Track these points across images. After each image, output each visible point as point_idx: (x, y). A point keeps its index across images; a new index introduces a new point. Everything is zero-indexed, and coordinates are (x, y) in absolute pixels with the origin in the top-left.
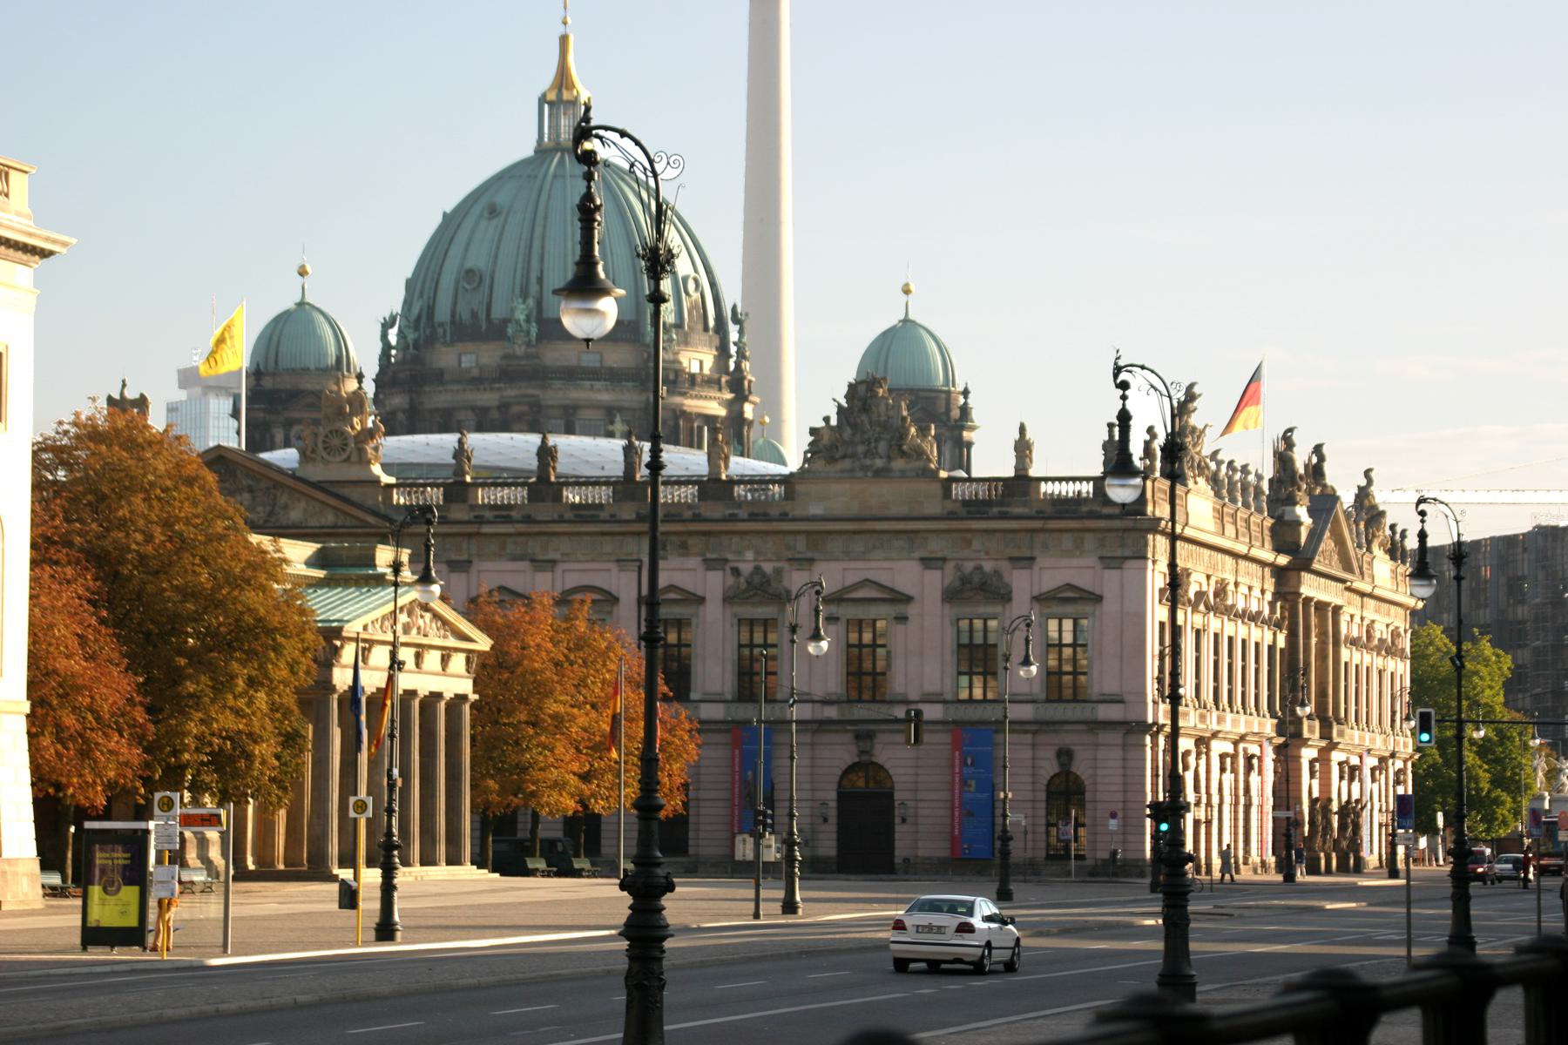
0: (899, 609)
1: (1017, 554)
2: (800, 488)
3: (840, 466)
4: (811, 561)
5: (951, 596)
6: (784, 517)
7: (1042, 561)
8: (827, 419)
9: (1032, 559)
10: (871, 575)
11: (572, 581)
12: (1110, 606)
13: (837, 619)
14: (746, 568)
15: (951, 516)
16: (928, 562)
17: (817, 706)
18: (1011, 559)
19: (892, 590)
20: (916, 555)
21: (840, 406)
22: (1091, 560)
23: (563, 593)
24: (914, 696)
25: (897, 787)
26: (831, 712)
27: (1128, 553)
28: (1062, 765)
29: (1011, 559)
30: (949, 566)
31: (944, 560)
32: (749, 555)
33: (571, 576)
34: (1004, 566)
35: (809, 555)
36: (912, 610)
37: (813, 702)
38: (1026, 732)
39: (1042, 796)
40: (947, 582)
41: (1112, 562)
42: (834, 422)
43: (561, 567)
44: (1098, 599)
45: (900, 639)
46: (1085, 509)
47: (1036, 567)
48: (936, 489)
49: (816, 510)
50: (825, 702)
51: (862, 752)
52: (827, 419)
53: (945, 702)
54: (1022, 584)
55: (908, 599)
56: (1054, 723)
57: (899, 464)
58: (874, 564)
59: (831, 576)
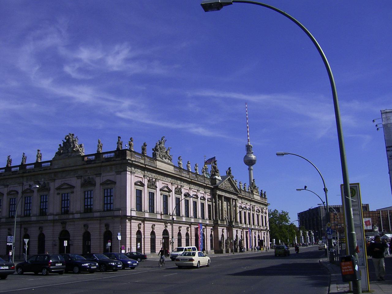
1: (98, 173)
2: (53, 162)
4: (55, 180)
5: (83, 185)
6: (50, 169)
7: (103, 175)
8: (60, 145)
9: (101, 174)
10: (66, 182)
11: (11, 189)
12: (118, 184)
13: (59, 194)
14: (42, 183)
15: (84, 164)
16: (78, 177)
17: (54, 216)
18: (96, 174)
19: (71, 185)
20: (76, 176)
21: (64, 142)
22: (113, 173)
23: (10, 191)
24: (74, 212)
25: (71, 236)
26: (57, 217)
27: (122, 170)
28: (106, 229)
29: (96, 174)
30: (82, 178)
31: (81, 176)
32: (43, 180)
33: (11, 188)
34: (94, 176)
36: (75, 190)
37: (54, 215)
38: (98, 220)
39: (102, 237)
41: (119, 173)
42: (62, 146)
43: (9, 186)
44: (115, 183)
45: (72, 197)
46: (112, 159)
47: (102, 176)
48: (80, 158)
49: (56, 167)
50: (56, 215)
51: (63, 228)
52: (60, 145)
53: (80, 213)
54: (98, 181)
55: (74, 187)
56: (104, 217)
58: (67, 179)
59: (58, 183)
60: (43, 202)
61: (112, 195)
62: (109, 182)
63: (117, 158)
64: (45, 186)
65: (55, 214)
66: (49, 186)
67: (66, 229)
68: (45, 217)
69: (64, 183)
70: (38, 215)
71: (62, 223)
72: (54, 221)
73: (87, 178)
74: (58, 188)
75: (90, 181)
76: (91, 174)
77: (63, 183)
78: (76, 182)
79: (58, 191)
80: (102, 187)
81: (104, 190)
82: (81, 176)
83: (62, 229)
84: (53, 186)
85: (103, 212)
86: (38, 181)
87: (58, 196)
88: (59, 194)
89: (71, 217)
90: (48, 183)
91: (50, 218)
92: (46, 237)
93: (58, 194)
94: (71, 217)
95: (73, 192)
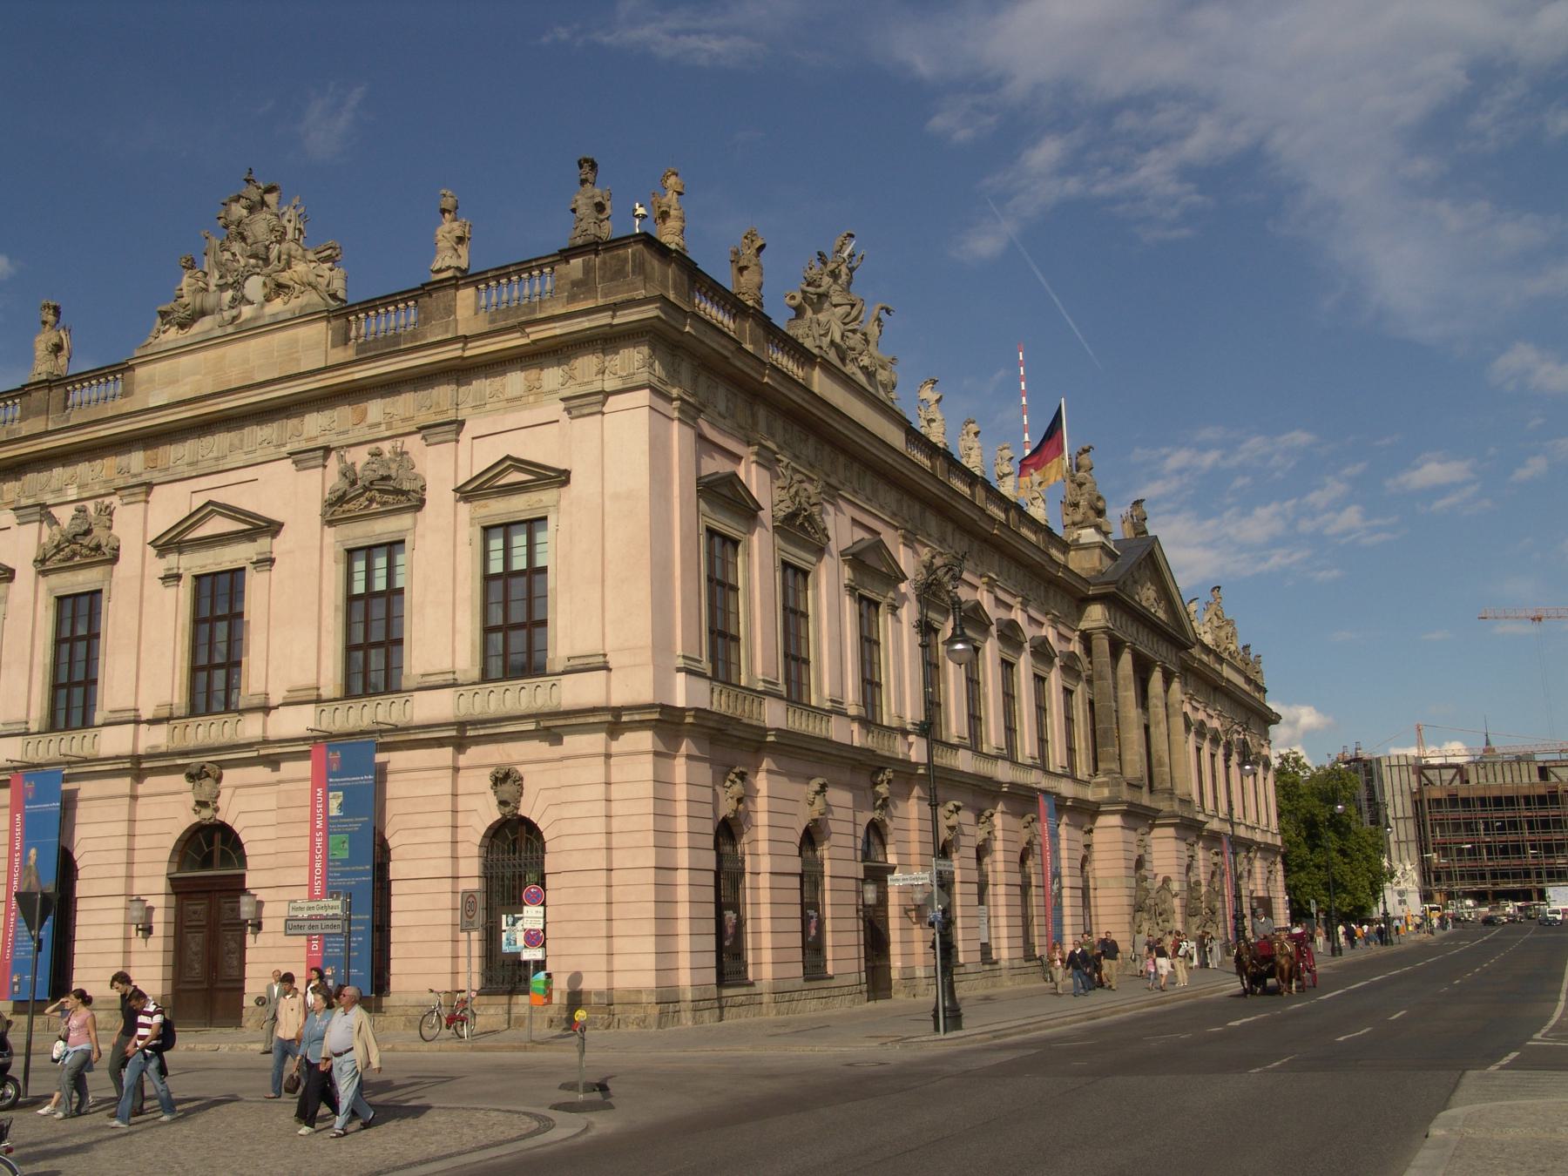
0: (262, 545)
3: (197, 328)
4: (149, 486)
5: (337, 509)
9: (462, 423)
13: (178, 577)
16: (300, 458)
22: (556, 409)
26: (155, 738)
31: (327, 450)
34: (414, 444)
35: (146, 478)
40: (329, 485)
47: (465, 436)
51: (202, 804)
54: (440, 469)
55: (272, 528)
57: (277, 306)
60: (73, 640)
61: (539, 563)
62: (516, 477)
63: (572, 298)
64: (88, 532)
65: (146, 714)
66: (110, 528)
67: (220, 817)
68: (78, 735)
69: (210, 503)
70: (34, 727)
71: (191, 777)
72: (137, 767)
73: (360, 457)
74: (169, 544)
75: (385, 478)
76: (389, 426)
77: (199, 501)
78: (286, 490)
79: (172, 560)
80: (464, 508)
81: (487, 530)
82: (327, 450)
83: (196, 819)
84: (134, 526)
85: (474, 683)
86: (43, 506)
87: (171, 591)
88: (178, 577)
89: (251, 727)
90: (109, 512)
91: (114, 742)
92: (81, 874)
93: (172, 578)
94: (251, 727)
95: (272, 561)
